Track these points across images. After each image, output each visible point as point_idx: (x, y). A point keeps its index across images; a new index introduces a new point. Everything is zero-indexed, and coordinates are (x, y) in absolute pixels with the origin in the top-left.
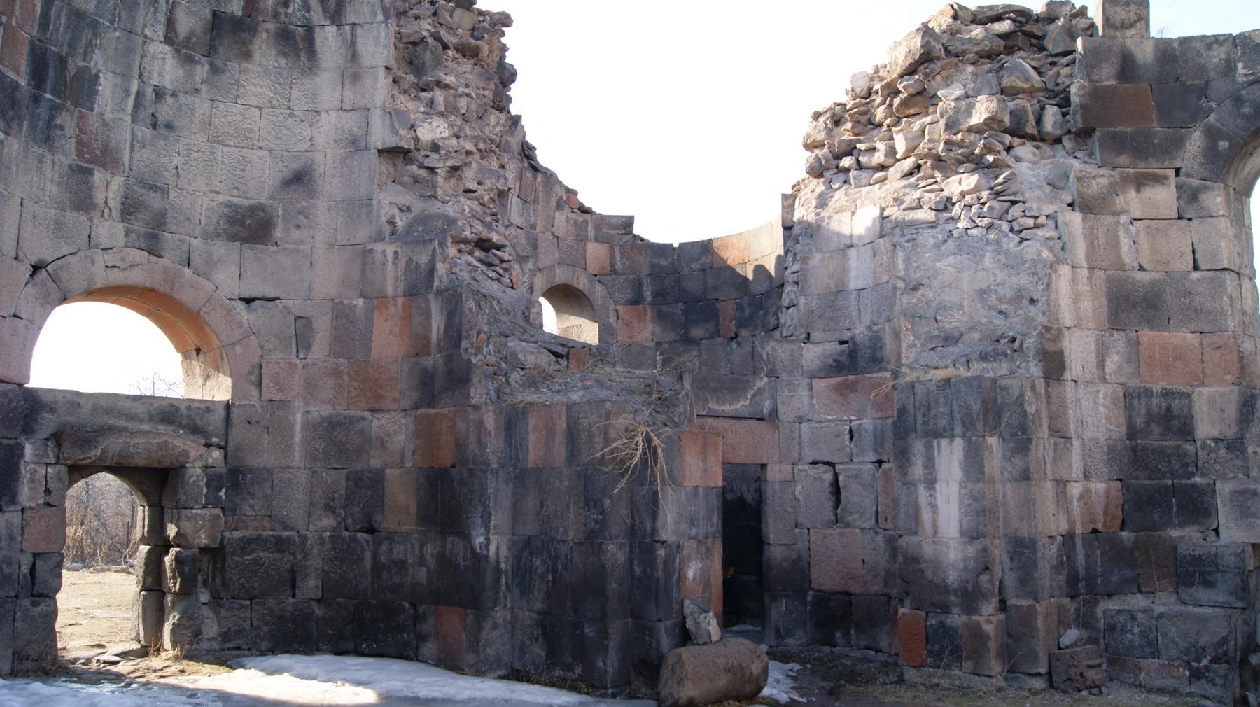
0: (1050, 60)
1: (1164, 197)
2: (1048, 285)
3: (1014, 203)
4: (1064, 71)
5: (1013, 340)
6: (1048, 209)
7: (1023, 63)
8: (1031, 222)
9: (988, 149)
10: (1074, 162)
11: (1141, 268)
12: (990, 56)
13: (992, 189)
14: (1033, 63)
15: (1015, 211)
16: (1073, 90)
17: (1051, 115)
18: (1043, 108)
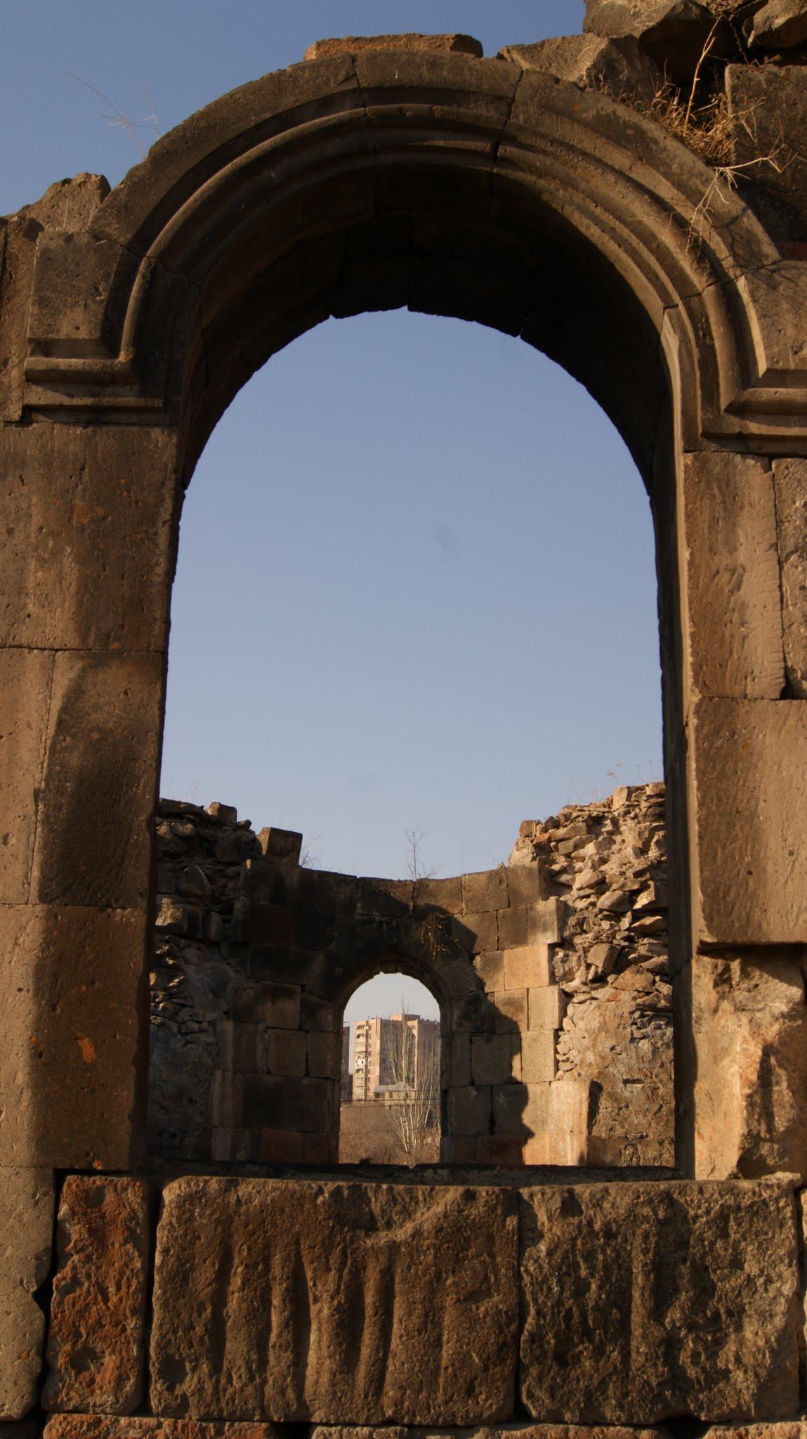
0: (219, 867)
1: (290, 1008)
2: (208, 1089)
3: (184, 1006)
4: (231, 884)
5: (173, 1136)
6: (210, 1016)
7: (201, 868)
8: (196, 1026)
9: (169, 954)
10: (228, 968)
11: (269, 1073)
12: (173, 856)
13: (165, 989)
14: (208, 872)
15: (184, 1014)
16: (238, 905)
17: (216, 918)
18: (209, 912)
